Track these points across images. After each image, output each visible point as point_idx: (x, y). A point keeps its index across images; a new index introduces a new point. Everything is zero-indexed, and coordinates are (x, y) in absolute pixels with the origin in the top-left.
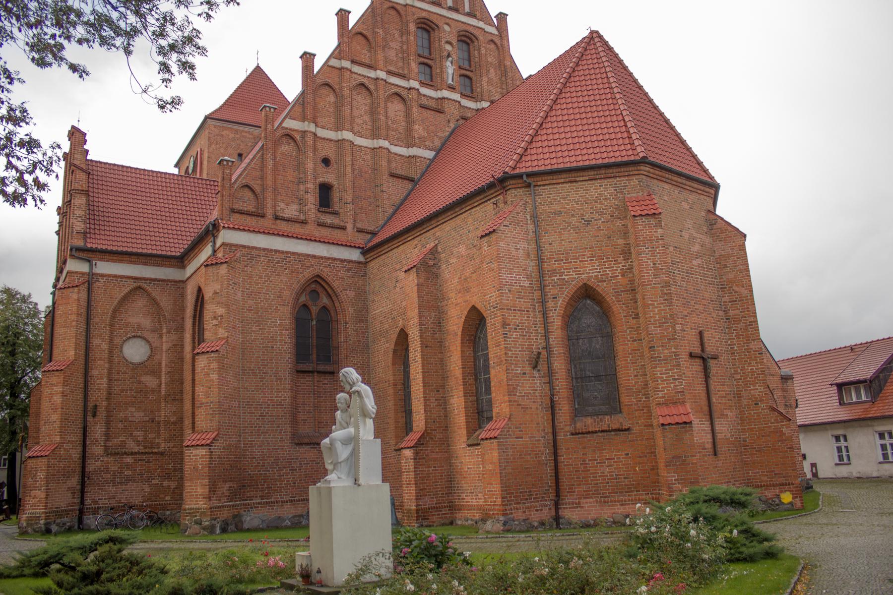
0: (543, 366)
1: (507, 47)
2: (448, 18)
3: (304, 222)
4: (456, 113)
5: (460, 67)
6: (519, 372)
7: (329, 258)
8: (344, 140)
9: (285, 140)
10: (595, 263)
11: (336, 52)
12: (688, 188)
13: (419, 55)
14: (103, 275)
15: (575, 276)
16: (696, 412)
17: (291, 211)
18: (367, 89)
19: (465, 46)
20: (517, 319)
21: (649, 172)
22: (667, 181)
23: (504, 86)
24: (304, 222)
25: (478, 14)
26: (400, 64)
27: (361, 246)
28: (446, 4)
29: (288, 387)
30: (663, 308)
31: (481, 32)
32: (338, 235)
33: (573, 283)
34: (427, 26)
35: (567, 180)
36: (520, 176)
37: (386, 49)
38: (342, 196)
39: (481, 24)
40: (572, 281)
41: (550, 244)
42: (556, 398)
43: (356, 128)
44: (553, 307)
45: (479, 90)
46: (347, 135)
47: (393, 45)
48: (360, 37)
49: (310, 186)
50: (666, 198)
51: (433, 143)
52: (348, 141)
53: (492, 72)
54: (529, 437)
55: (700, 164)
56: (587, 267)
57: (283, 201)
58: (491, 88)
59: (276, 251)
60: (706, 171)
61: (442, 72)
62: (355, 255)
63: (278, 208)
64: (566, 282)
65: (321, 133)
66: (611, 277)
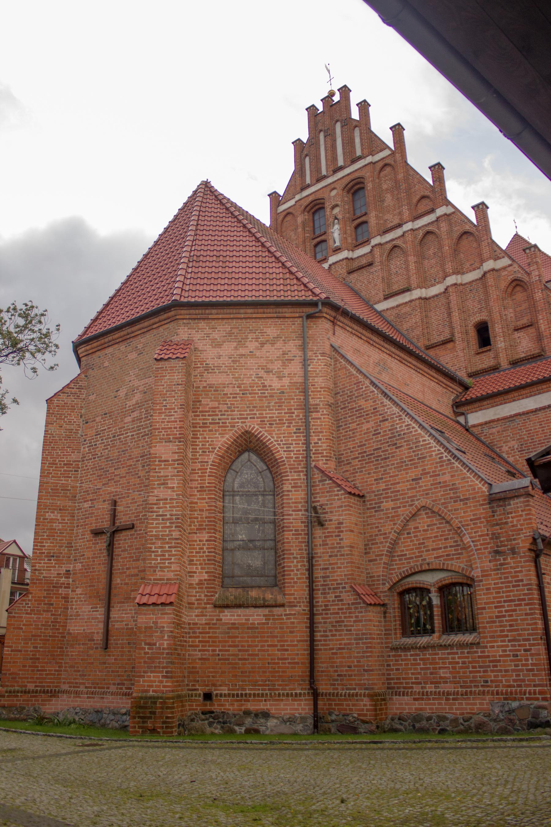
2: (331, 184)
12: (139, 332)
16: (90, 597)
21: (87, 351)
22: (110, 344)
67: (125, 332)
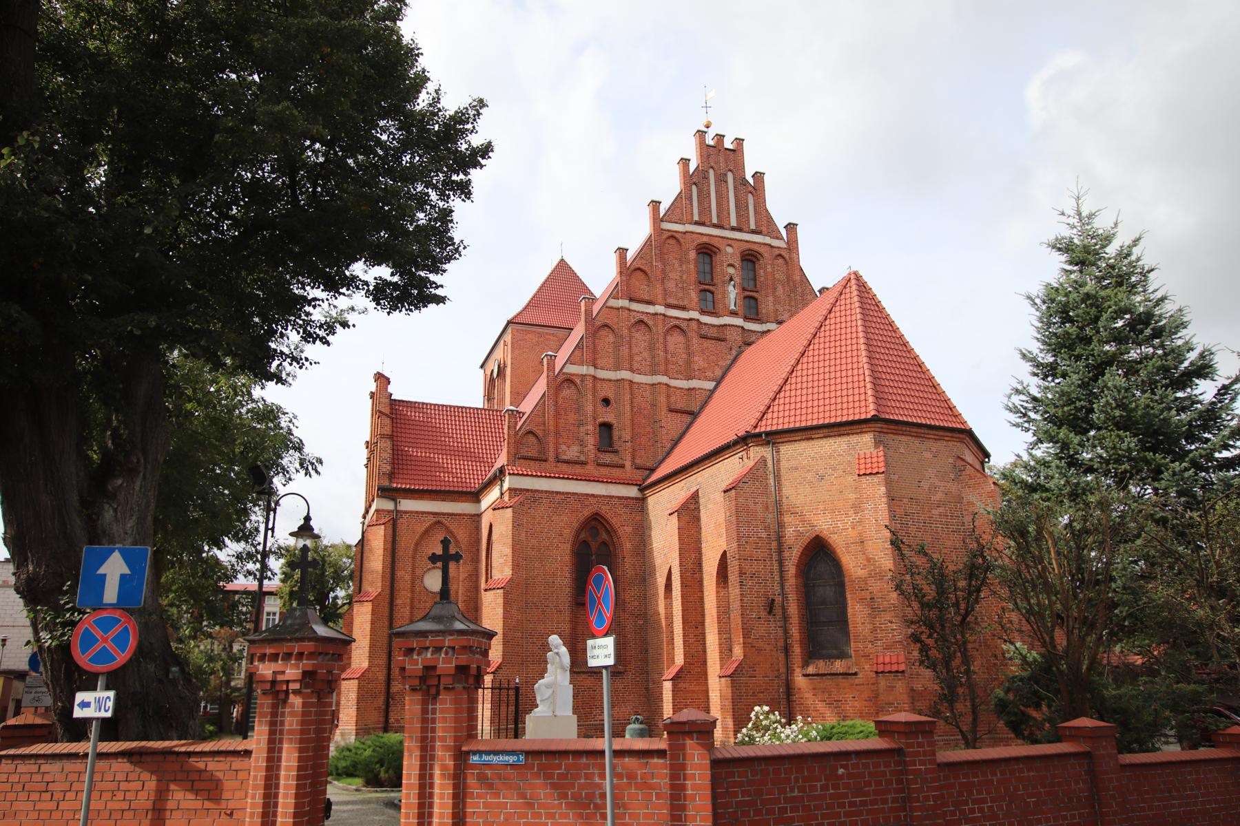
0: (778, 610)
3: (583, 463)
4: (739, 339)
5: (744, 289)
7: (607, 496)
8: (623, 379)
9: (566, 385)
11: (614, 292)
12: (933, 437)
13: (700, 283)
14: (406, 512)
17: (572, 453)
18: (646, 325)
19: (750, 264)
21: (882, 428)
24: (583, 463)
25: (764, 229)
26: (680, 295)
27: (639, 483)
28: (729, 224)
29: (568, 619)
31: (767, 248)
32: (616, 472)
34: (707, 251)
35: (804, 437)
36: (759, 435)
38: (623, 433)
39: (767, 240)
42: (789, 641)
43: (636, 366)
45: (764, 311)
46: (625, 374)
47: (673, 275)
48: (639, 273)
49: (590, 427)
50: (902, 450)
52: (627, 380)
54: (763, 677)
55: (951, 408)
57: (565, 443)
59: (557, 493)
60: (957, 416)
62: (633, 492)
63: (560, 451)
65: (602, 374)
67: (922, 431)
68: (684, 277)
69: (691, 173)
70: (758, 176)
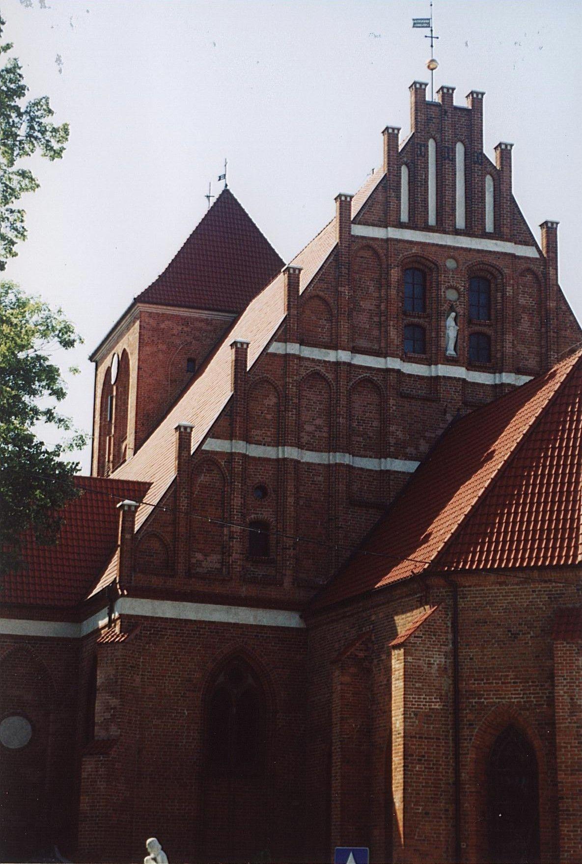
1: (552, 277)
5: (470, 322)
6: (420, 811)
10: (519, 687)
11: (280, 332)
15: (495, 700)
20: (423, 749)
23: (543, 343)
25: (506, 230)
26: (375, 333)
30: (576, 752)
33: (493, 708)
37: (355, 314)
40: (492, 706)
41: (471, 659)
43: (305, 439)
44: (468, 735)
45: (499, 355)
47: (366, 305)
51: (417, 448)
53: (525, 324)
56: (510, 691)
58: (520, 348)
61: (438, 336)
63: (194, 561)
64: (485, 706)
66: (535, 705)
68: (383, 307)
69: (400, 149)
70: (505, 151)
